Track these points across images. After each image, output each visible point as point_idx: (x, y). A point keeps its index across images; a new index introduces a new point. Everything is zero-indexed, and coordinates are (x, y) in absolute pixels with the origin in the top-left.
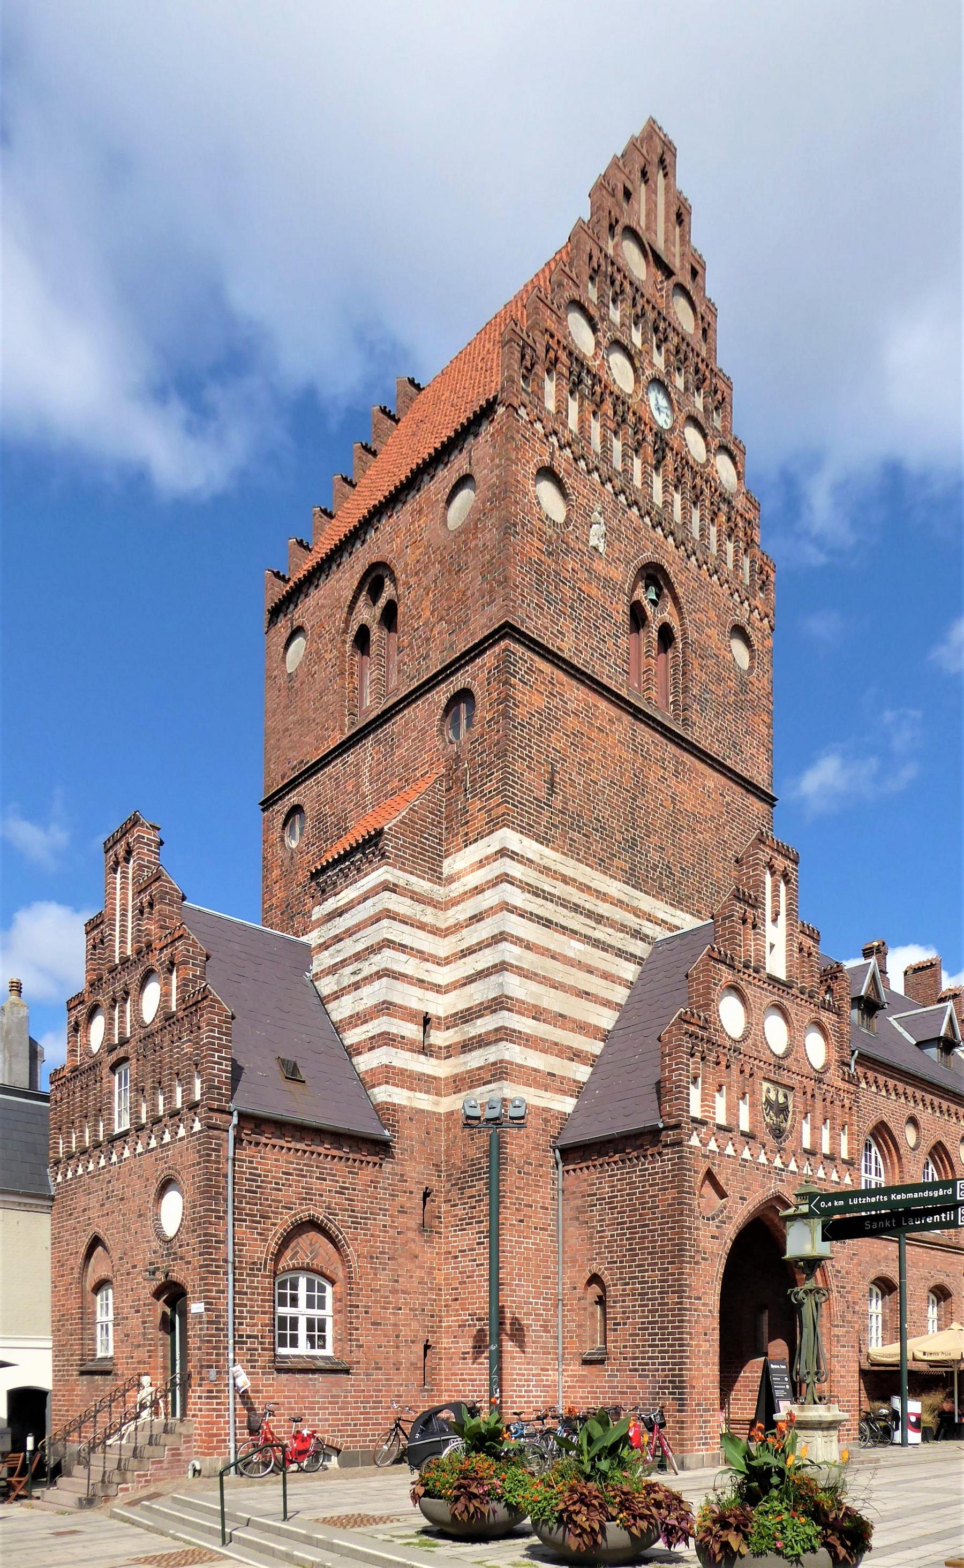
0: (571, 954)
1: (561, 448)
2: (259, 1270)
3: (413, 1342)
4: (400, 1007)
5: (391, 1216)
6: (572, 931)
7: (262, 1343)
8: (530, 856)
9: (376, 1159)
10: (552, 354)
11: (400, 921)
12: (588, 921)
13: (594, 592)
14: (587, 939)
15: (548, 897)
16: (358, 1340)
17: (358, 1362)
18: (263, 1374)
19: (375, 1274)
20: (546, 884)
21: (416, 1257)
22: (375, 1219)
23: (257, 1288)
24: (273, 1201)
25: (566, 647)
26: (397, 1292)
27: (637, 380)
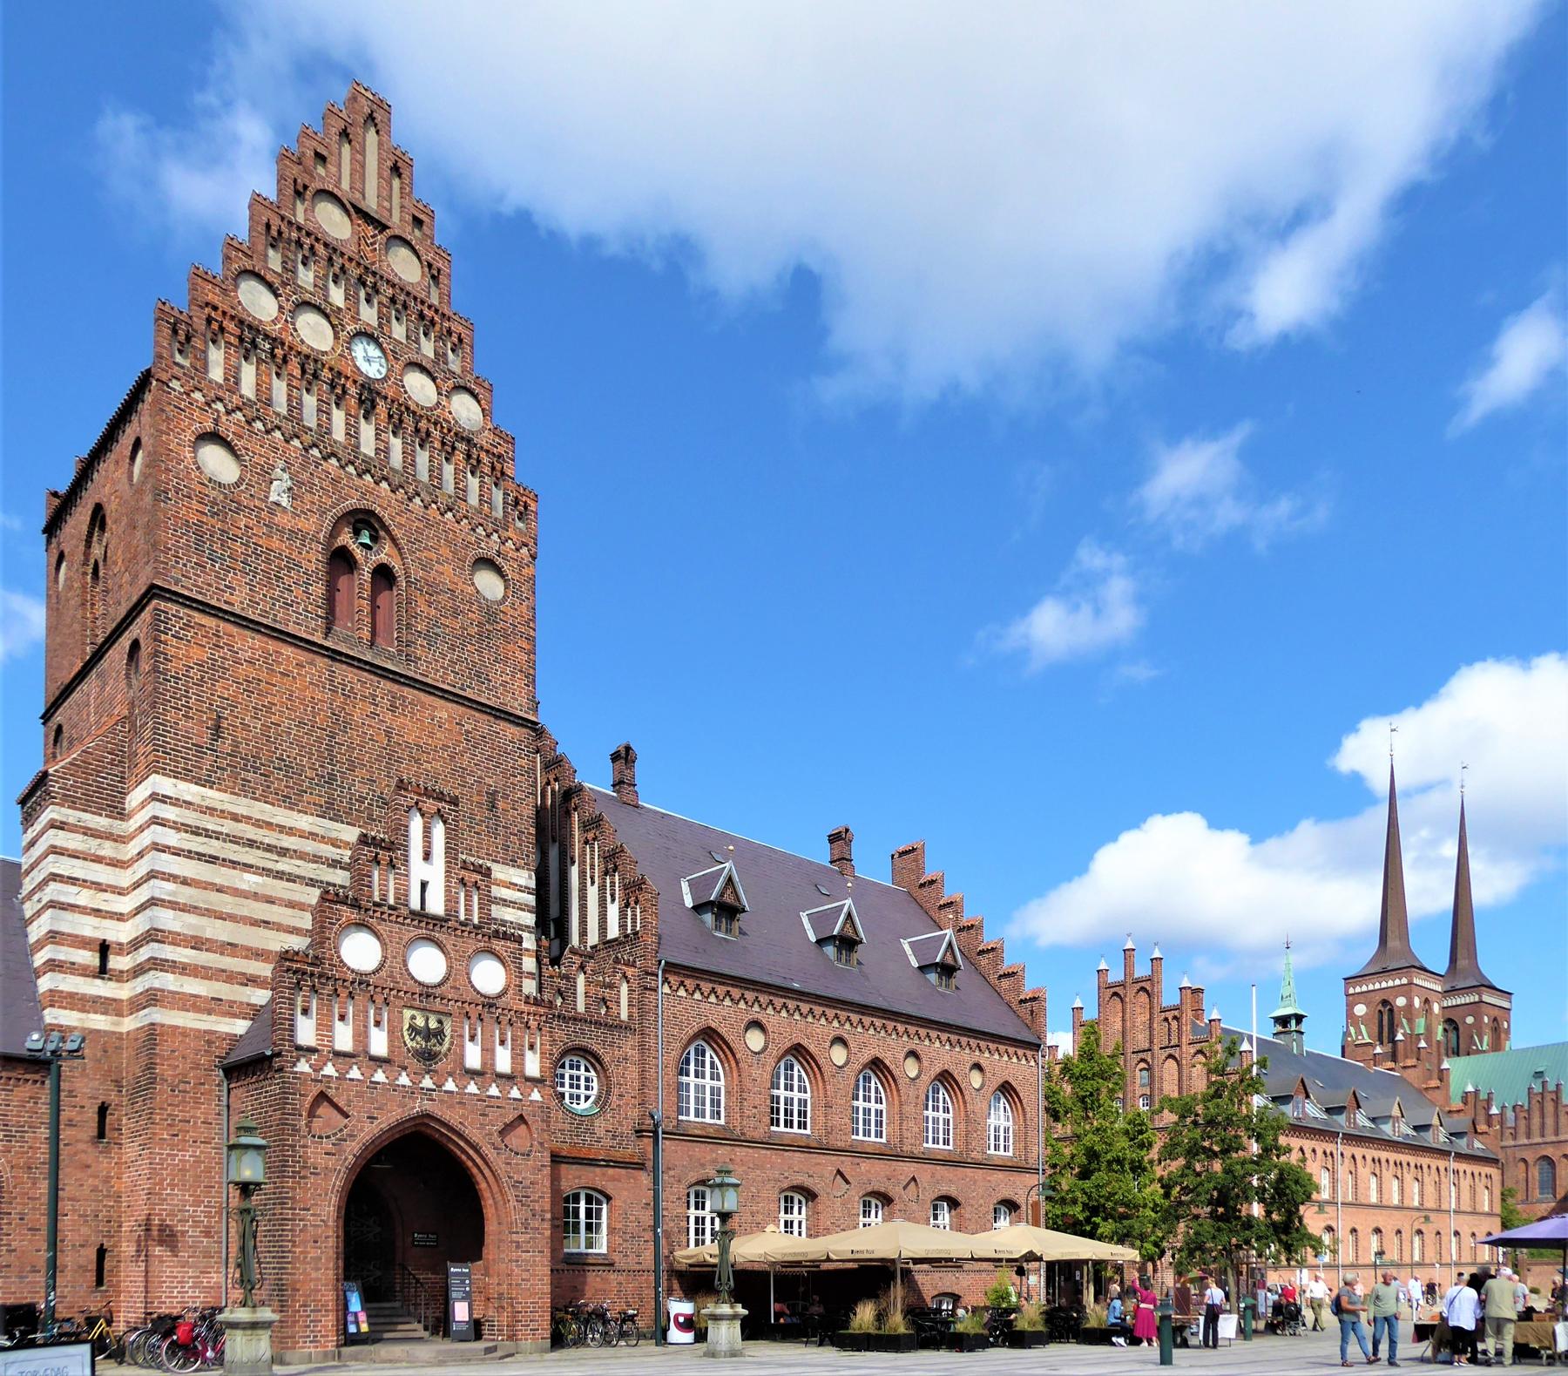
0: (245, 887)
1: (228, 413)
6: (245, 865)
8: (188, 798)
10: (215, 326)
12: (268, 855)
13: (275, 544)
14: (266, 872)
15: (208, 834)
20: (210, 824)
25: (238, 601)
27: (336, 337)
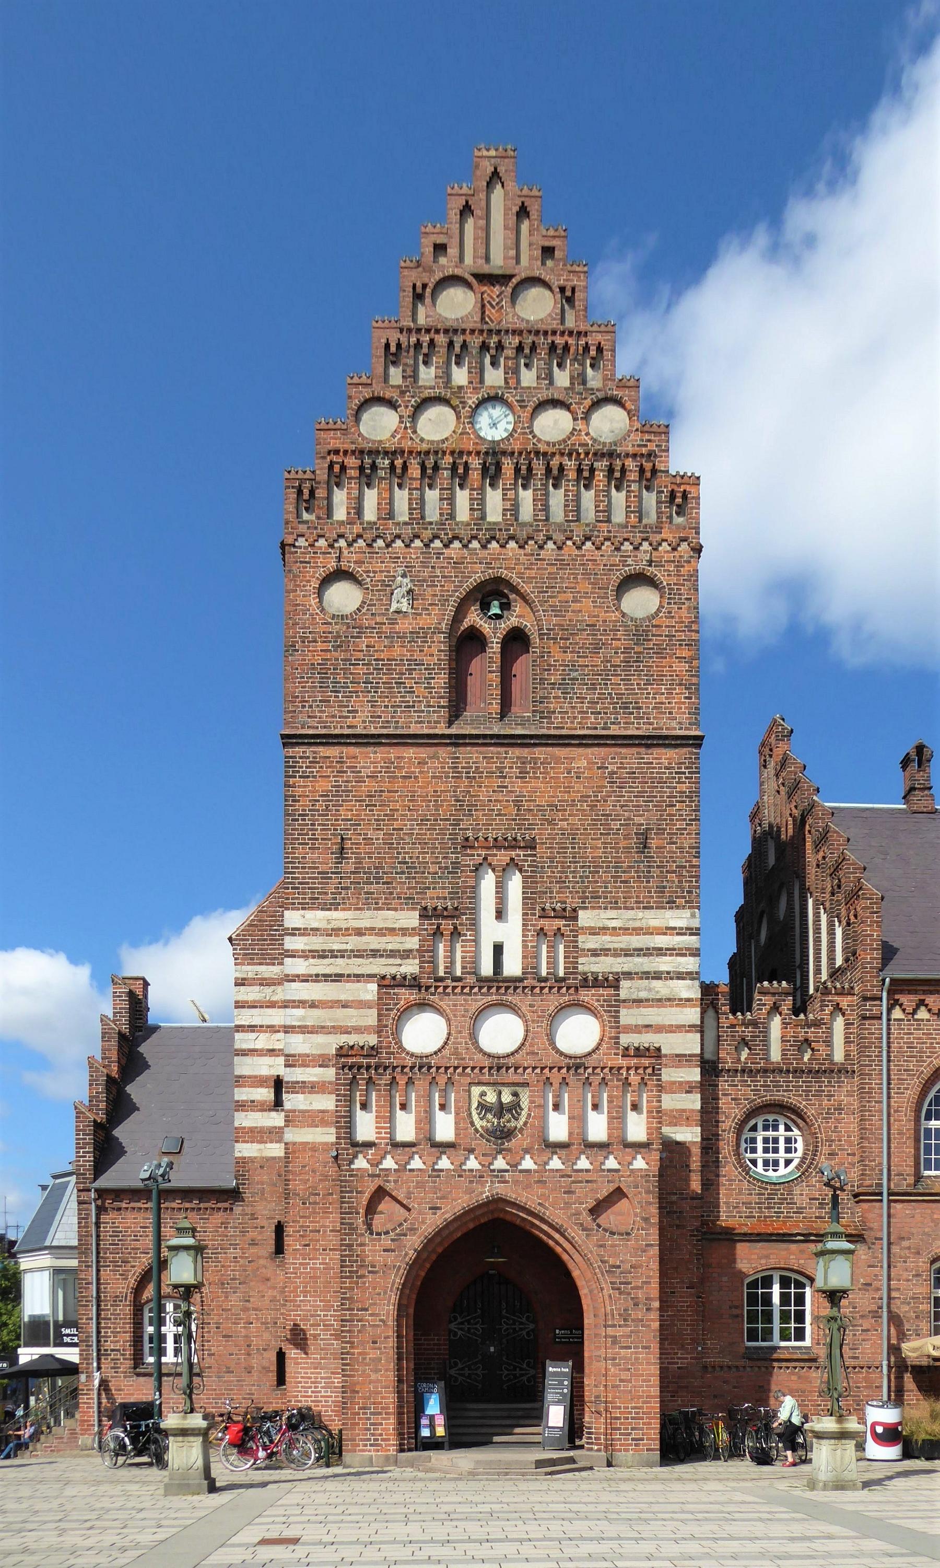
2: (121, 1301)
3: (265, 1350)
4: (250, 1077)
5: (242, 1249)
7: (123, 1355)
9: (226, 1205)
11: (249, 1007)
16: (210, 1350)
17: (210, 1367)
18: (125, 1377)
19: (227, 1297)
21: (268, 1280)
22: (225, 1253)
23: (119, 1314)
24: (132, 1249)
26: (248, 1309)
